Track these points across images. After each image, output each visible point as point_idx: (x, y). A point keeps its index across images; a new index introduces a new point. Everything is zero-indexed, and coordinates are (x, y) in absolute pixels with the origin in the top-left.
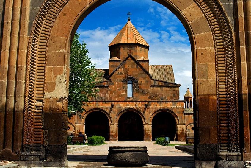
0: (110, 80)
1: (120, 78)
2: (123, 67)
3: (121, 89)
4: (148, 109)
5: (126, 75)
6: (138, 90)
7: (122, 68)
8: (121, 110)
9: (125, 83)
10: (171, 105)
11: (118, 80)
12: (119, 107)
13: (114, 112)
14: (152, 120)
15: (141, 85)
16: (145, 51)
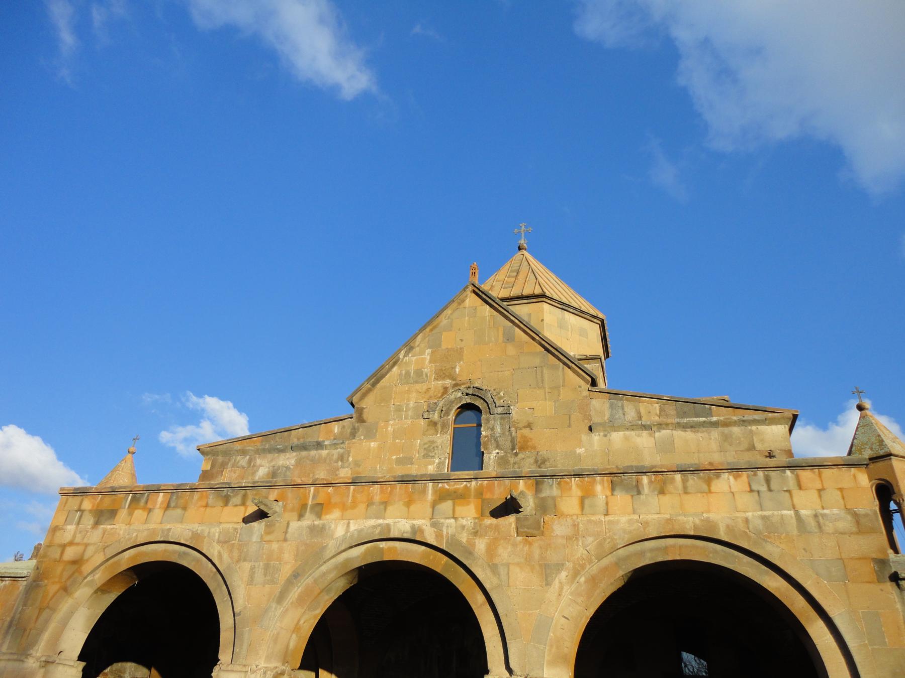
0: (360, 412)
1: (415, 399)
2: (435, 345)
3: (409, 460)
4: (537, 542)
5: (448, 382)
6: (512, 460)
7: (428, 351)
8: (323, 548)
9: (435, 424)
10: (745, 500)
11: (399, 409)
12: (312, 529)
13: (267, 567)
14: (571, 646)
15: (529, 426)
16: (583, 333)
